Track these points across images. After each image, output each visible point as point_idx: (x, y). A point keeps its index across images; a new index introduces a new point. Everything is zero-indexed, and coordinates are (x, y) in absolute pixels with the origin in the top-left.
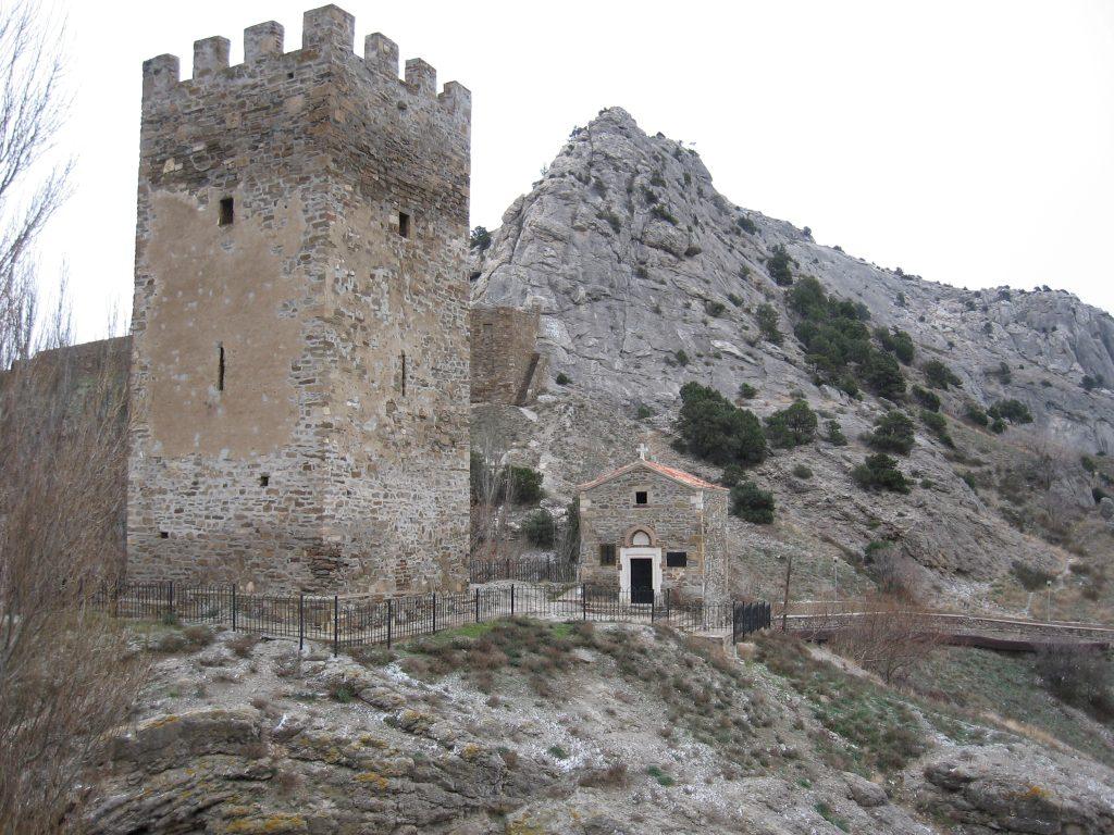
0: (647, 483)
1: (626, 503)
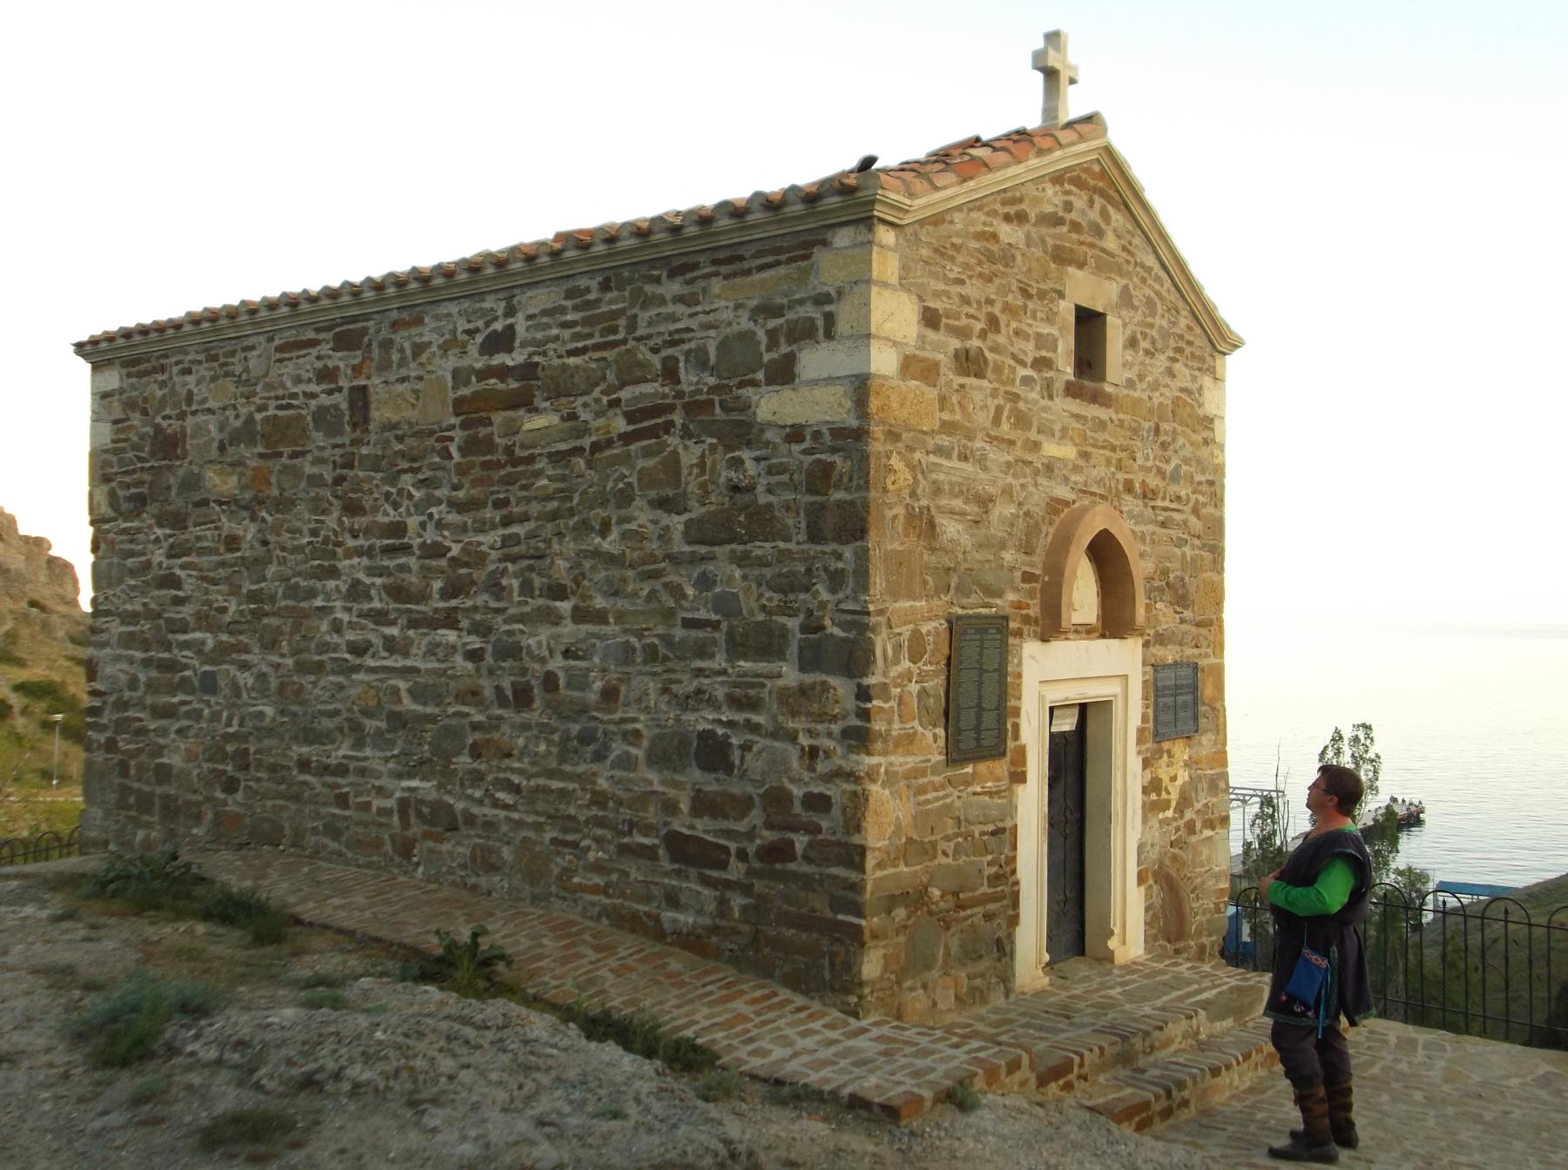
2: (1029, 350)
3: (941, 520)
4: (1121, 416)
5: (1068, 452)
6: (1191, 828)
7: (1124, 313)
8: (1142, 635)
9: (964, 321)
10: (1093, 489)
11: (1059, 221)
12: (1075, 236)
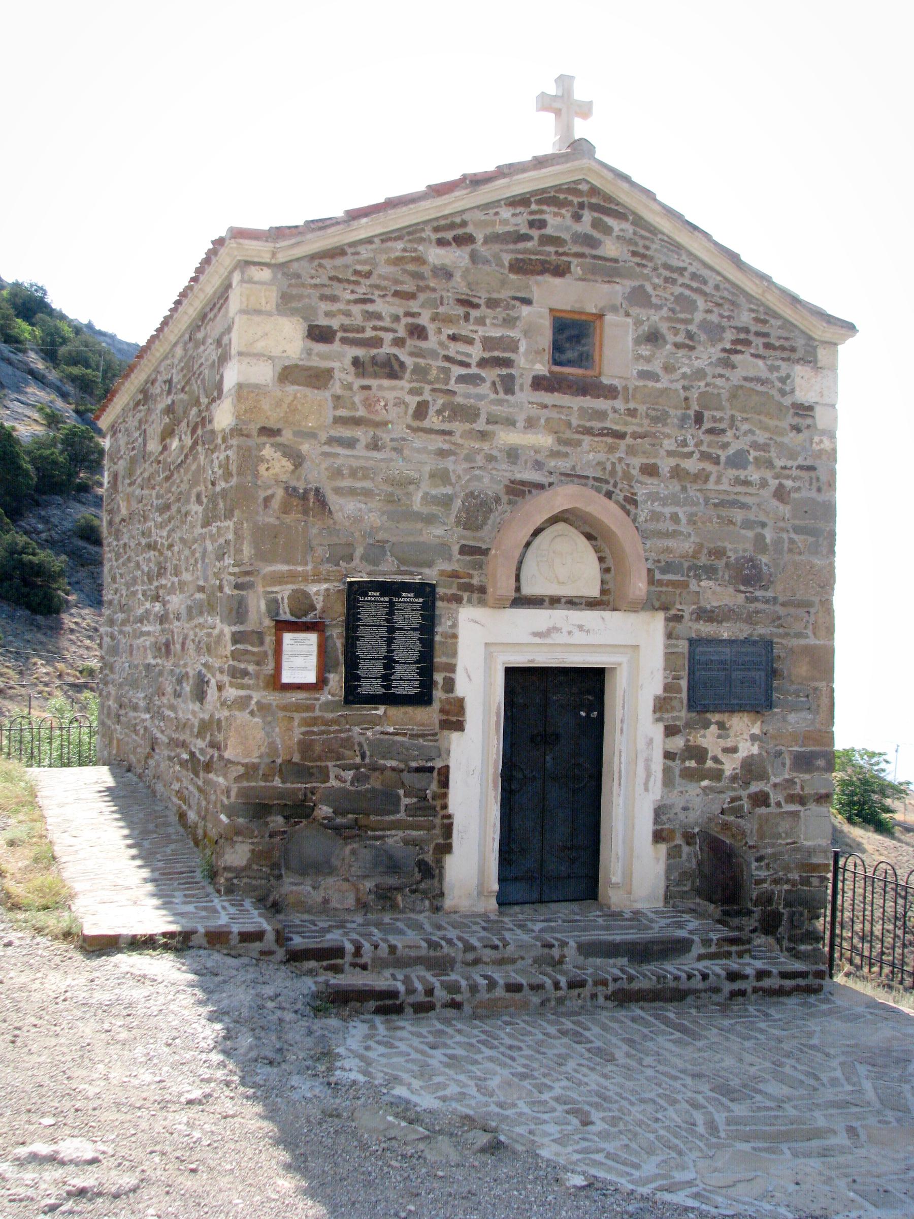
0: (608, 270)
1: (499, 359)
2: (476, 352)
3: (333, 500)
4: (632, 405)
5: (545, 440)
6: (761, 799)
7: (635, 311)
8: (665, 608)
9: (369, 333)
10: (590, 473)
11: (527, 238)
12: (551, 249)
